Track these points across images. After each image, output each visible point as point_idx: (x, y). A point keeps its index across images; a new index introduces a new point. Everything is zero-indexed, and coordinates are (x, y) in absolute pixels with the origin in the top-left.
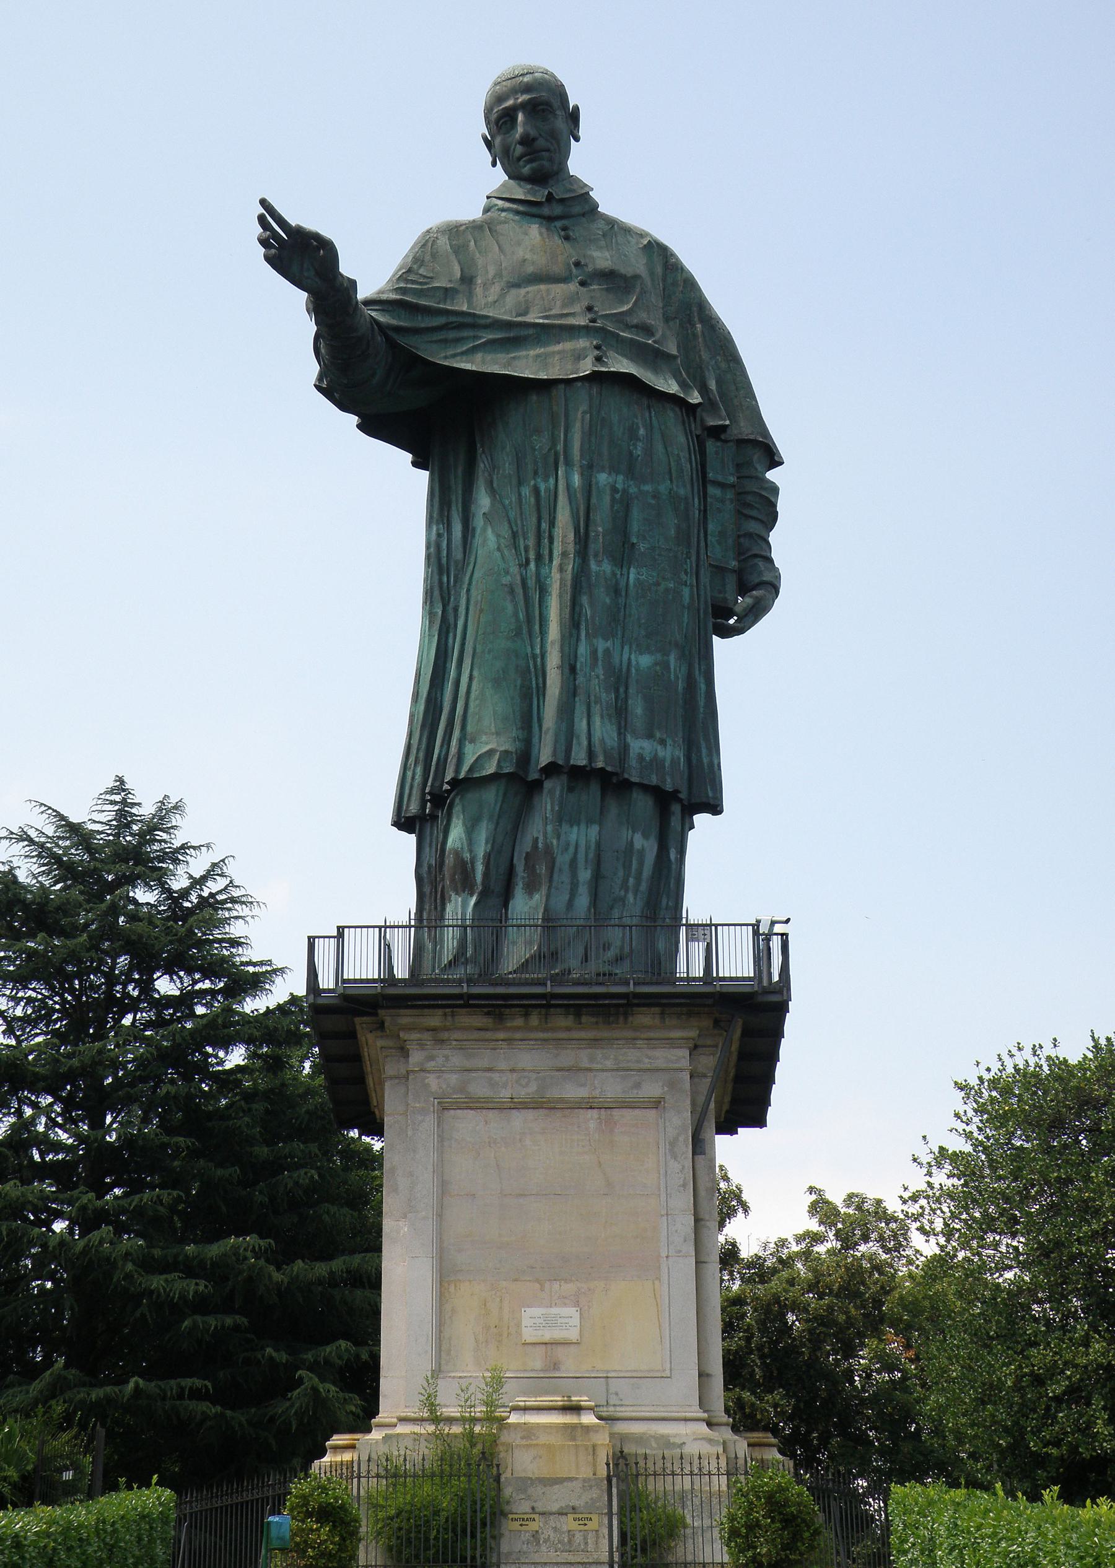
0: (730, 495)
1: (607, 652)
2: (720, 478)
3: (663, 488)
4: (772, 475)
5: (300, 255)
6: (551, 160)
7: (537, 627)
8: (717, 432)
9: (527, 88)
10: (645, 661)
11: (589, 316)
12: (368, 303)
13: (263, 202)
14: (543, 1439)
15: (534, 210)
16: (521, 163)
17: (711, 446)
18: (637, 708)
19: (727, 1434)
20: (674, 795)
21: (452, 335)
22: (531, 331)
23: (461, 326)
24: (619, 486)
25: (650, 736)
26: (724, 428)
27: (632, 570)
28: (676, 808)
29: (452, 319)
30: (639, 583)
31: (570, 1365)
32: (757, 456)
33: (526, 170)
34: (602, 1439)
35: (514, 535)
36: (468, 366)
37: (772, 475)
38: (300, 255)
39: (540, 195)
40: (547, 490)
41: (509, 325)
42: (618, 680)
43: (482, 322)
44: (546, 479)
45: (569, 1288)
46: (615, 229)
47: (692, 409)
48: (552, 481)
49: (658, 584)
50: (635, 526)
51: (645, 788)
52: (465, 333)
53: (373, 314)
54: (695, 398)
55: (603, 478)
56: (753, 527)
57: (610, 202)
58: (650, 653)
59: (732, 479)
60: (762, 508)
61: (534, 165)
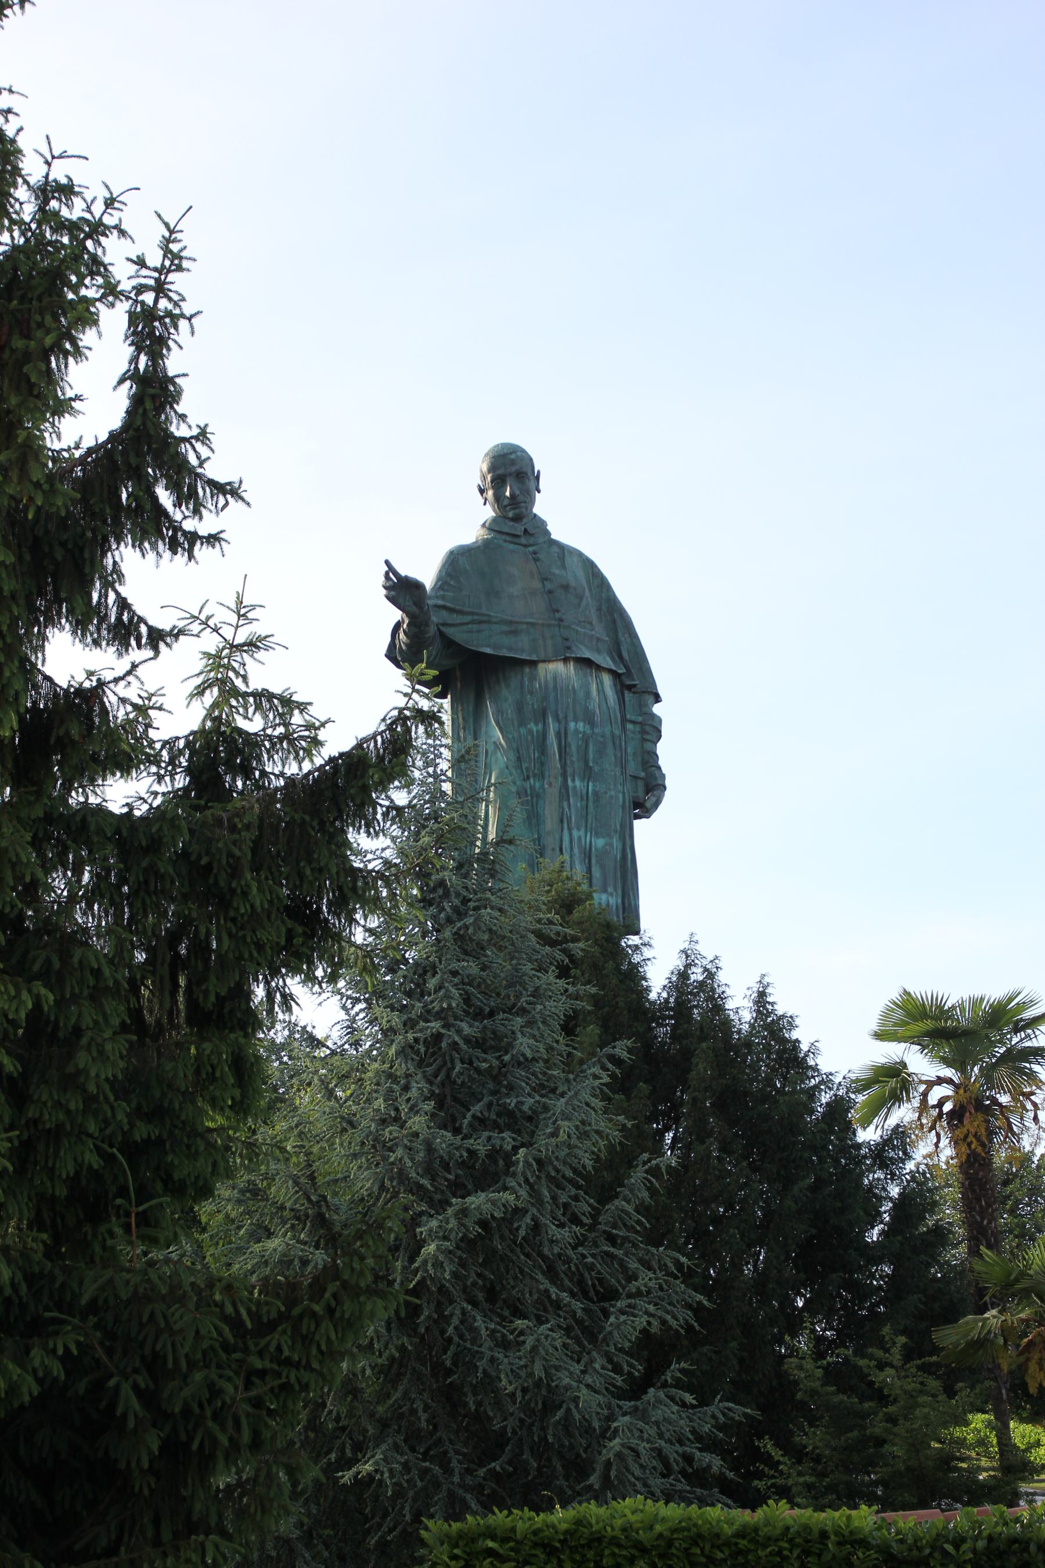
0: (638, 728)
1: (580, 838)
2: (633, 718)
3: (607, 730)
4: (657, 709)
6: (526, 508)
7: (534, 821)
8: (630, 688)
9: (513, 462)
10: (600, 842)
11: (557, 615)
13: (387, 562)
15: (517, 540)
16: (508, 509)
17: (627, 694)
18: (596, 873)
21: (475, 627)
22: (525, 627)
23: (481, 622)
24: (581, 729)
25: (605, 891)
26: (635, 686)
27: (591, 784)
29: (476, 617)
30: (596, 793)
32: (651, 699)
33: (511, 514)
35: (519, 759)
36: (488, 651)
37: (657, 709)
39: (519, 529)
40: (537, 731)
41: (511, 622)
42: (587, 855)
43: (494, 620)
44: (536, 724)
46: (563, 551)
48: (540, 726)
49: (606, 793)
50: (591, 756)
52: (484, 626)
54: (622, 670)
55: (572, 725)
56: (648, 746)
57: (558, 532)
58: (603, 837)
59: (640, 719)
60: (652, 730)
61: (517, 511)
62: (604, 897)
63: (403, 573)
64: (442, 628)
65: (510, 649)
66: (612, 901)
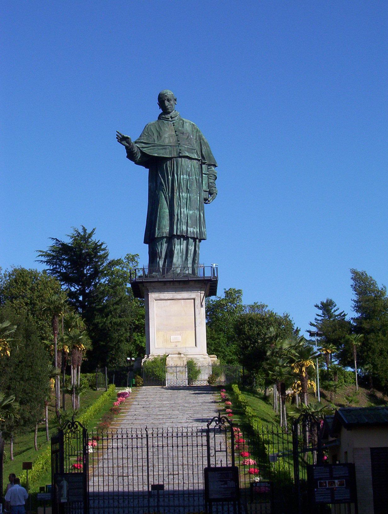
5: (123, 139)
10: (191, 212)
12: (136, 142)
14: (175, 359)
18: (189, 222)
19: (207, 356)
20: (197, 238)
28: (198, 240)
31: (179, 346)
34: (185, 359)
36: (156, 155)
38: (123, 139)
45: (179, 332)
47: (199, 160)
51: (191, 238)
53: (137, 145)
62: (192, 229)
63: (122, 134)
64: (141, 149)
65: (163, 154)
66: (195, 230)
